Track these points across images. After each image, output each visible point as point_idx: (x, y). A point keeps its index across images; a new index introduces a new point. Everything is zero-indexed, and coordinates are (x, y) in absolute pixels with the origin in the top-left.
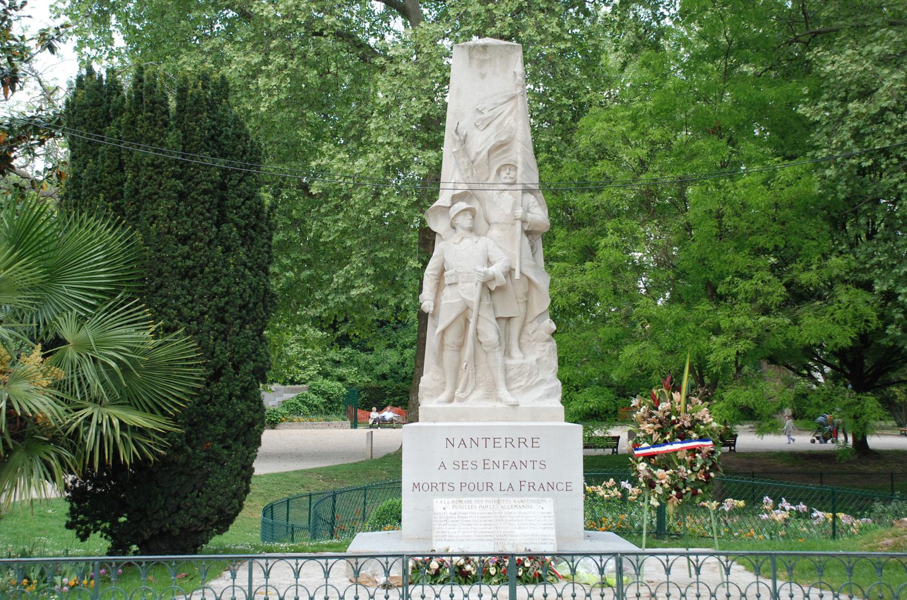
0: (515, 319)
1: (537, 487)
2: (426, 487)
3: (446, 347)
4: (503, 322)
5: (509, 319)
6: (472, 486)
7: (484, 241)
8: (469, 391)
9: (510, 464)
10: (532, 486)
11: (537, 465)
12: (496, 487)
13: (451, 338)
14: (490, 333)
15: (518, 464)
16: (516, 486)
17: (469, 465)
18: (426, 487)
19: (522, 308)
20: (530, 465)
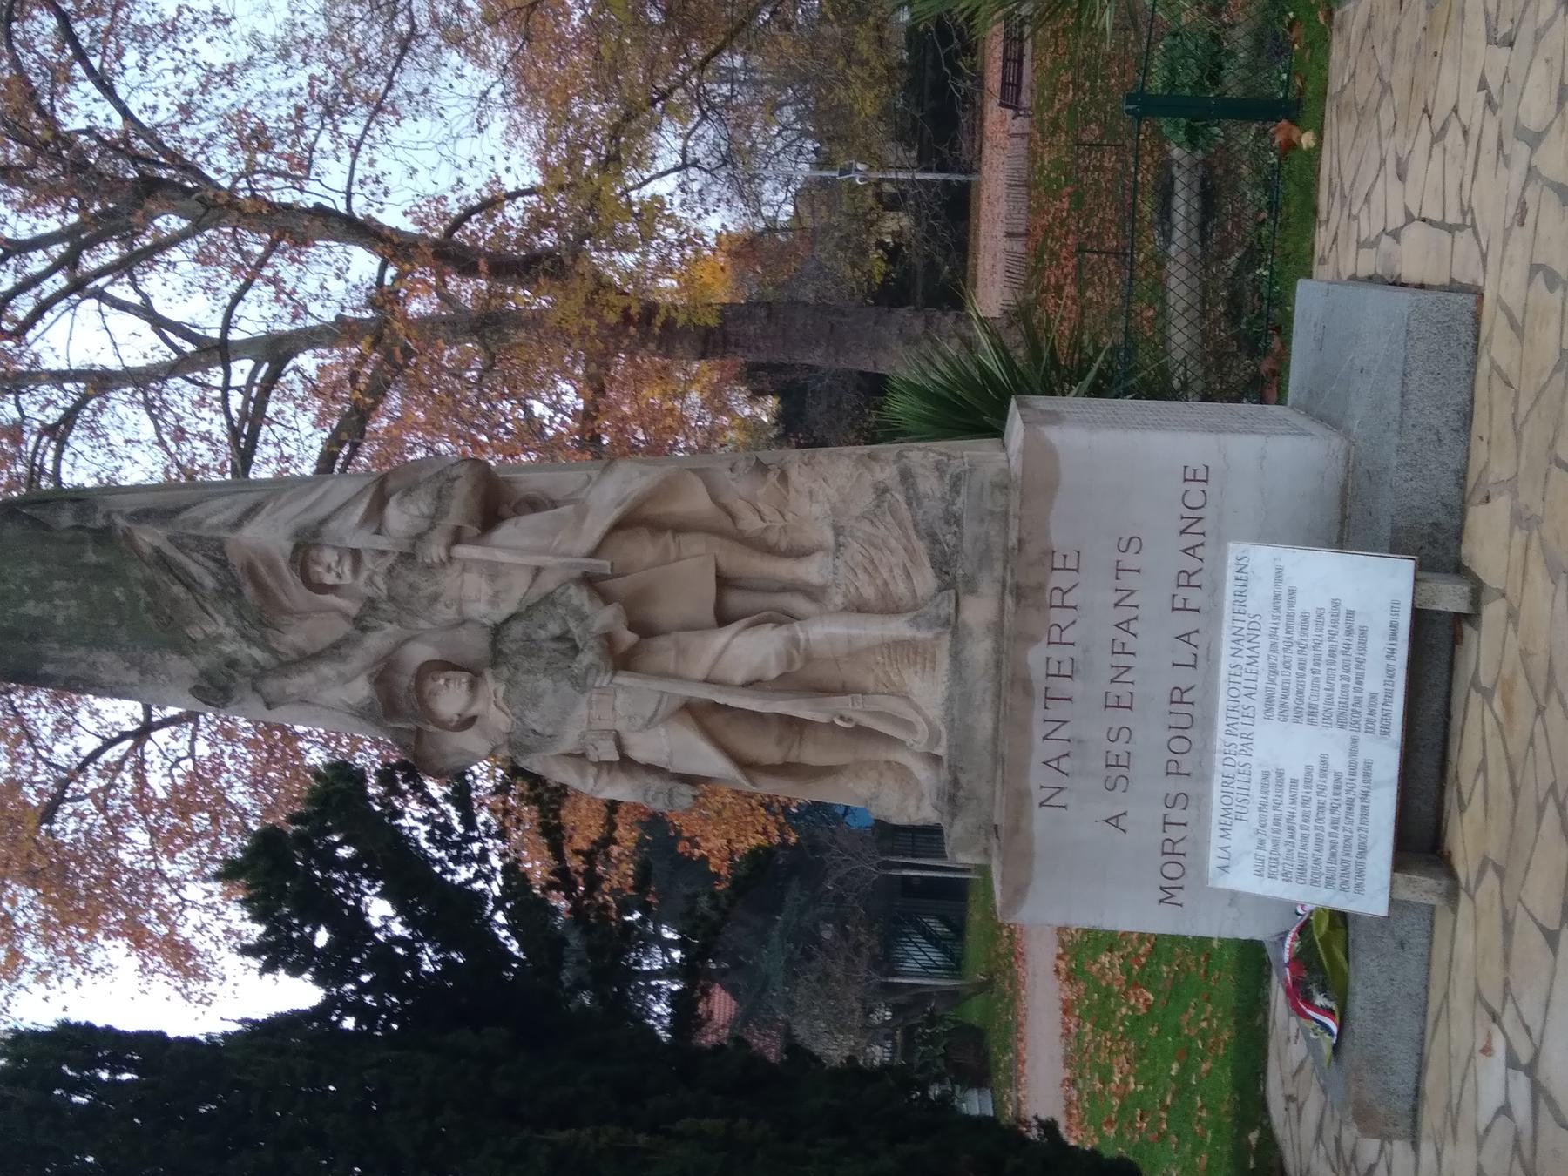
0: (724, 565)
1: (1190, 564)
2: (1172, 871)
3: (792, 758)
4: (736, 600)
5: (724, 582)
6: (1178, 745)
7: (825, 174)
8: (911, 716)
9: (1124, 637)
10: (1186, 579)
11: (1129, 560)
12: (1184, 678)
13: (767, 750)
14: (751, 650)
15: (1125, 614)
16: (1186, 622)
17: (1119, 748)
18: (1172, 871)
19: (695, 545)
20: (1128, 580)
